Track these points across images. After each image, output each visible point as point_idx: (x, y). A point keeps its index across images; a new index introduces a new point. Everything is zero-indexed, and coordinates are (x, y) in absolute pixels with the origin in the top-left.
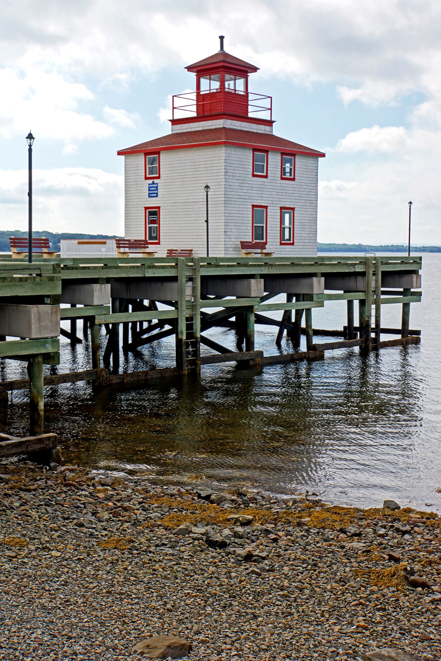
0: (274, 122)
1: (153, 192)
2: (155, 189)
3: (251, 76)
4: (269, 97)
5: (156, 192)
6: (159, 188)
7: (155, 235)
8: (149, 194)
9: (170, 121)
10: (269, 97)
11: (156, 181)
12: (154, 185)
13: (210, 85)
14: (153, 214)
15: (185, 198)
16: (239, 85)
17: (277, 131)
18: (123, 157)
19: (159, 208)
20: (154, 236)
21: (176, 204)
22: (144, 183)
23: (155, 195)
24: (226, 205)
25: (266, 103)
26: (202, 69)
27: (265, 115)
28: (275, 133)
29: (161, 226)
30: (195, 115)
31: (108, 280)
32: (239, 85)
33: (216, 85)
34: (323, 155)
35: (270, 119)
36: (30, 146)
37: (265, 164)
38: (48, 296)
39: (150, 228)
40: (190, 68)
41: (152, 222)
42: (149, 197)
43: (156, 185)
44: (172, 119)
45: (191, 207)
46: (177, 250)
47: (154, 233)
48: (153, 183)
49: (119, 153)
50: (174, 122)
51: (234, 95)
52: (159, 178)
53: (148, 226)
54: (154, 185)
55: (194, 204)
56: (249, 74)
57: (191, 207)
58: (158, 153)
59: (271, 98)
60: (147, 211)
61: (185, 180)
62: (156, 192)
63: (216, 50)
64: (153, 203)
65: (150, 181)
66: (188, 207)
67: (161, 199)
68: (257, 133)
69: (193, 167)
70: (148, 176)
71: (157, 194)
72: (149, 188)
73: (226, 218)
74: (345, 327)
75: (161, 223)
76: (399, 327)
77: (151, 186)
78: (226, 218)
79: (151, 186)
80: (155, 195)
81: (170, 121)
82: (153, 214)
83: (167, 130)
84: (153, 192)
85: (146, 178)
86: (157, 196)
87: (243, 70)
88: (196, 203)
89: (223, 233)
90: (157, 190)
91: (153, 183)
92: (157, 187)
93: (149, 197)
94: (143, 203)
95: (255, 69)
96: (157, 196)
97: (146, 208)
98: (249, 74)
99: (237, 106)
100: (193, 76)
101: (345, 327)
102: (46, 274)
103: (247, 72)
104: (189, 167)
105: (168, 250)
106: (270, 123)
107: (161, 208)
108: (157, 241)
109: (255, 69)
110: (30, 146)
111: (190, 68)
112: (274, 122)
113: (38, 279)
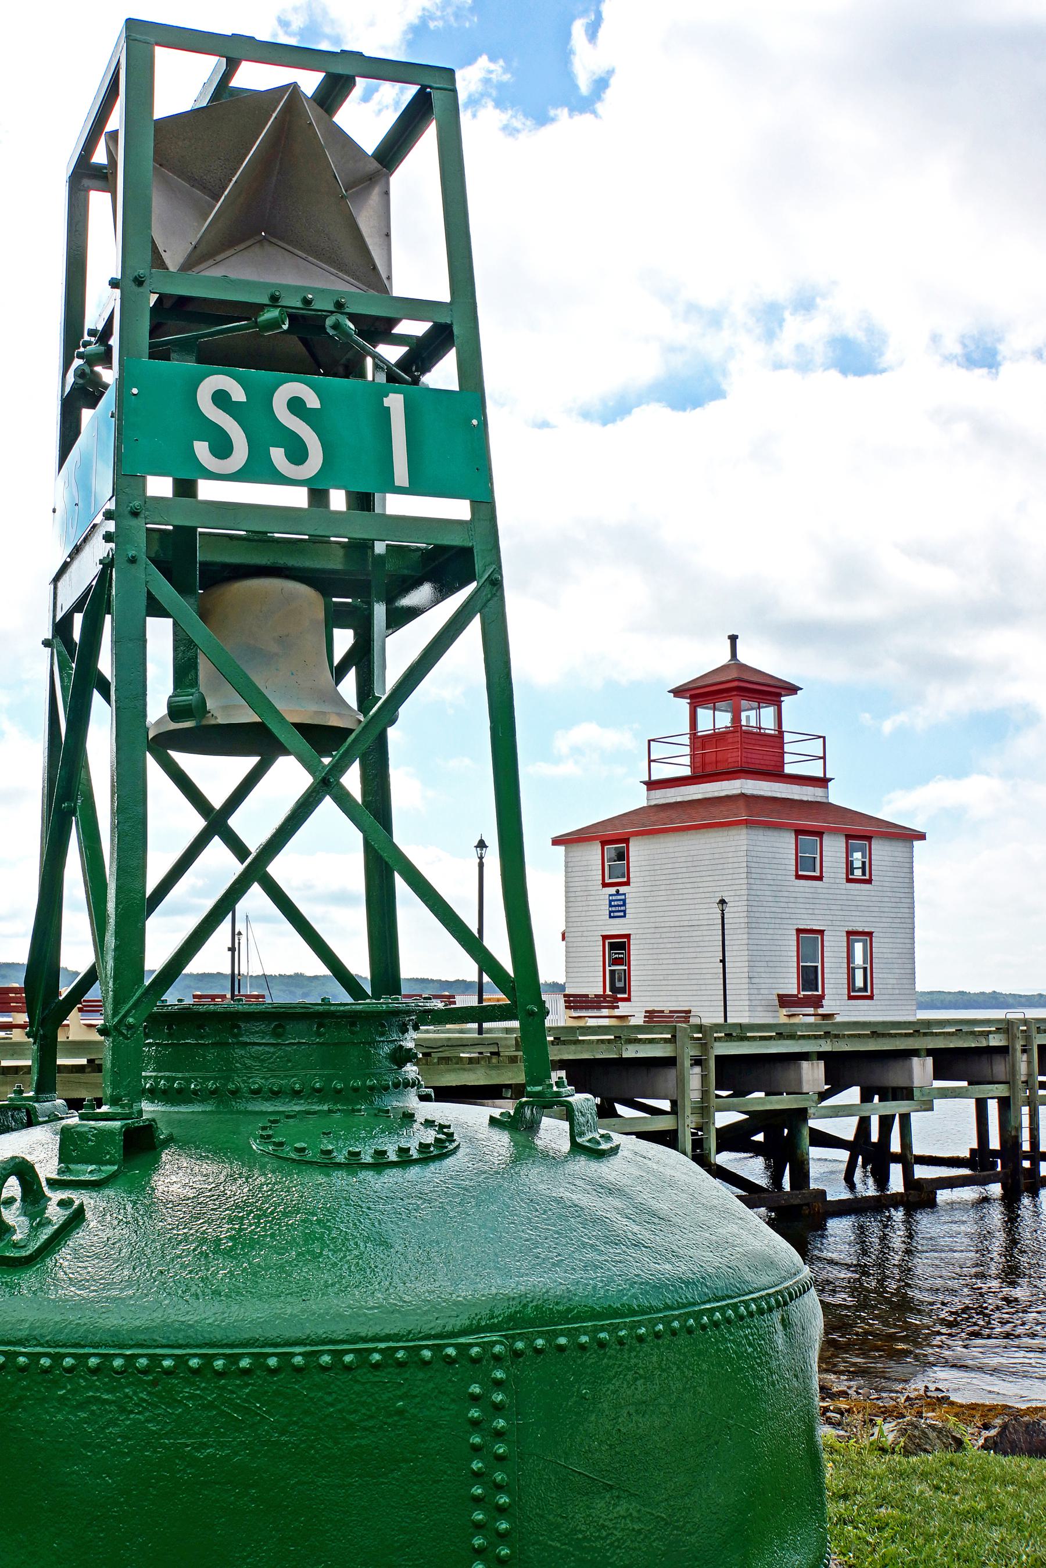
0: (831, 780)
1: (618, 909)
2: (621, 903)
3: (788, 702)
4: (820, 737)
5: (623, 908)
8: (610, 912)
9: (645, 783)
10: (820, 737)
11: (623, 889)
12: (619, 897)
13: (714, 720)
14: (618, 948)
15: (676, 918)
16: (764, 718)
17: (837, 796)
18: (561, 849)
19: (628, 936)
20: (619, 988)
21: (660, 930)
22: (600, 892)
23: (622, 914)
24: (751, 931)
26: (699, 693)
27: (814, 770)
29: (632, 968)
30: (687, 772)
32: (764, 718)
33: (724, 720)
34: (922, 837)
35: (822, 775)
36: (481, 858)
37: (818, 856)
38: (508, 1086)
39: (612, 972)
40: (678, 692)
41: (616, 962)
42: (610, 917)
43: (623, 897)
44: (647, 779)
45: (687, 934)
46: (662, 1012)
47: (620, 980)
48: (618, 891)
49: (556, 842)
50: (652, 785)
51: (758, 737)
52: (627, 883)
53: (608, 969)
54: (619, 897)
55: (692, 928)
56: (782, 699)
57: (687, 934)
58: (627, 841)
59: (824, 738)
60: (607, 942)
61: (675, 887)
62: (623, 908)
63: (725, 658)
64: (617, 927)
65: (612, 890)
66: (682, 934)
67: (632, 921)
69: (690, 864)
70: (607, 881)
71: (624, 911)
72: (610, 901)
73: (750, 953)
75: (632, 963)
77: (614, 898)
78: (750, 953)
79: (614, 898)
80: (622, 914)
81: (645, 783)
82: (618, 948)
83: (639, 799)
84: (618, 909)
85: (605, 885)
86: (624, 916)
87: (772, 691)
88: (696, 928)
89: (747, 980)
90: (624, 905)
91: (618, 891)
92: (624, 901)
93: (610, 917)
94: (599, 928)
95: (793, 690)
96: (624, 916)
97: (605, 938)
98: (782, 699)
99: (764, 755)
100: (684, 704)
102: (506, 1053)
103: (781, 695)
104: (681, 865)
105: (646, 1012)
106: (823, 782)
108: (626, 996)
109: (793, 690)
110: (481, 858)
111: (678, 692)
112: (831, 780)
113: (494, 1060)
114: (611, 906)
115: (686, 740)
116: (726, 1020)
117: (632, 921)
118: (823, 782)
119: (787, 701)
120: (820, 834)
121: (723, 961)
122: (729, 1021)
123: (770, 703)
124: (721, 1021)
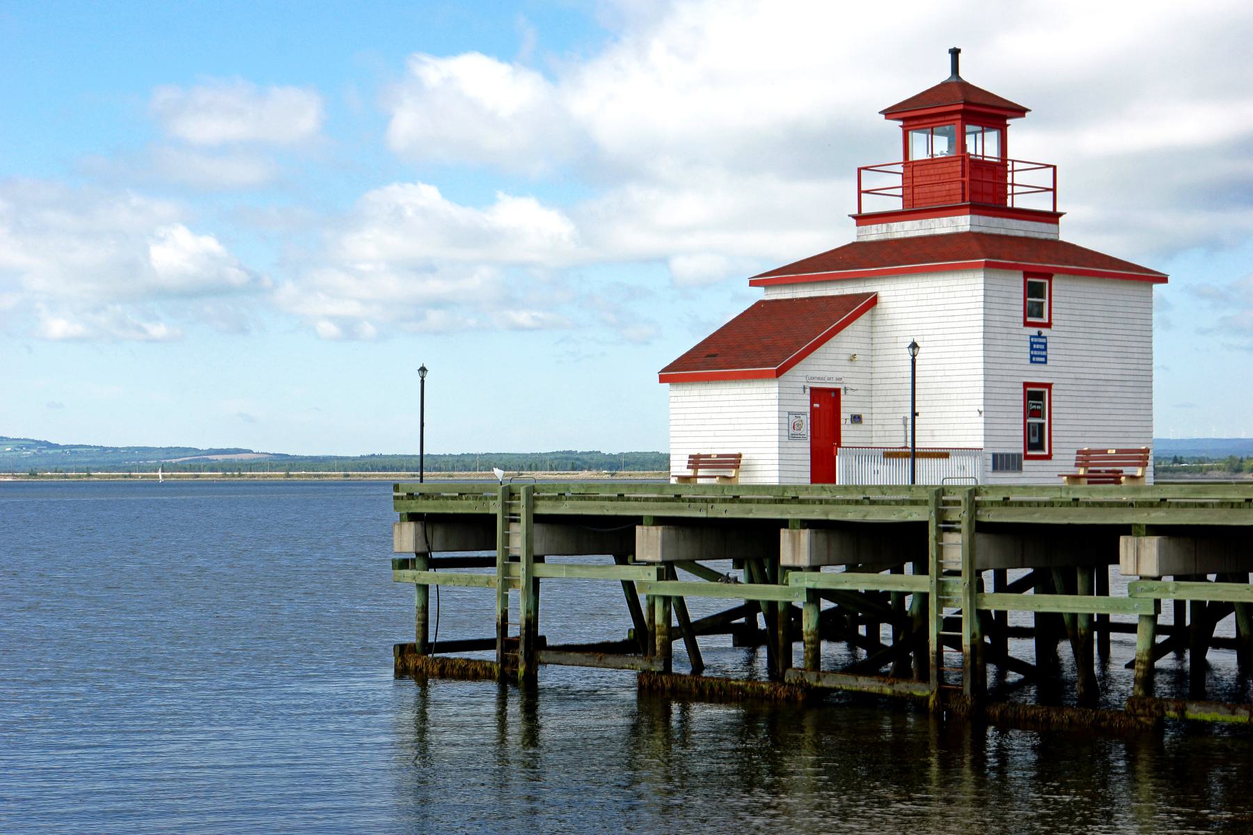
0: (1061, 215)
1: (1038, 352)
3: (1014, 126)
4: (1048, 166)
6: (1049, 345)
8: (1032, 356)
10: (1048, 166)
11: (1045, 331)
12: (1041, 340)
13: (932, 146)
14: (1035, 397)
16: (984, 145)
17: (1067, 233)
19: (1049, 386)
20: (1036, 441)
25: (1045, 178)
26: (913, 114)
27: (1042, 203)
28: (1064, 237)
30: (897, 205)
31: (1153, 530)
32: (984, 145)
33: (941, 146)
34: (1163, 279)
35: (1051, 209)
37: (1047, 301)
40: (889, 113)
42: (1032, 362)
48: (1040, 333)
51: (979, 165)
52: (1049, 325)
54: (1041, 340)
56: (1008, 122)
59: (1055, 168)
63: (945, 74)
64: (1038, 375)
65: (1034, 331)
67: (1053, 369)
68: (1007, 236)
72: (1032, 344)
74: (544, 638)
76: (492, 634)
82: (1035, 397)
84: (1038, 352)
86: (1045, 362)
87: (995, 113)
91: (1040, 333)
92: (1045, 344)
95: (1020, 112)
98: (1008, 122)
99: (985, 185)
100: (896, 126)
101: (544, 638)
103: (1006, 118)
106: (1053, 217)
107: (1053, 387)
109: (1020, 112)
111: (889, 113)
112: (1061, 215)
114: (1032, 349)
115: (900, 169)
116: (913, 481)
117: (1053, 369)
118: (1053, 217)
119: (1013, 125)
120: (1049, 276)
121: (914, 414)
122: (919, 482)
123: (991, 127)
124: (908, 482)
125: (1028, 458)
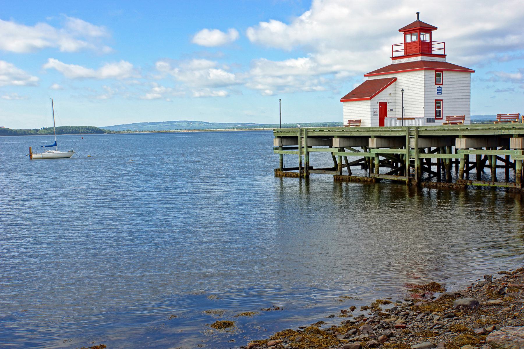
1: (439, 92)
7: (438, 114)
11: (441, 86)
13: (412, 38)
14: (438, 103)
16: (425, 37)
17: (448, 60)
19: (442, 100)
20: (438, 115)
26: (407, 30)
27: (441, 52)
30: (403, 54)
32: (425, 37)
33: (414, 38)
40: (400, 30)
51: (424, 43)
52: (442, 84)
58: (442, 72)
64: (439, 97)
65: (438, 86)
82: (438, 103)
84: (439, 92)
85: (436, 84)
87: (429, 29)
95: (435, 28)
99: (426, 48)
106: (444, 56)
109: (435, 28)
111: (400, 30)
118: (444, 56)
119: (434, 32)
123: (428, 33)
125: (436, 119)
